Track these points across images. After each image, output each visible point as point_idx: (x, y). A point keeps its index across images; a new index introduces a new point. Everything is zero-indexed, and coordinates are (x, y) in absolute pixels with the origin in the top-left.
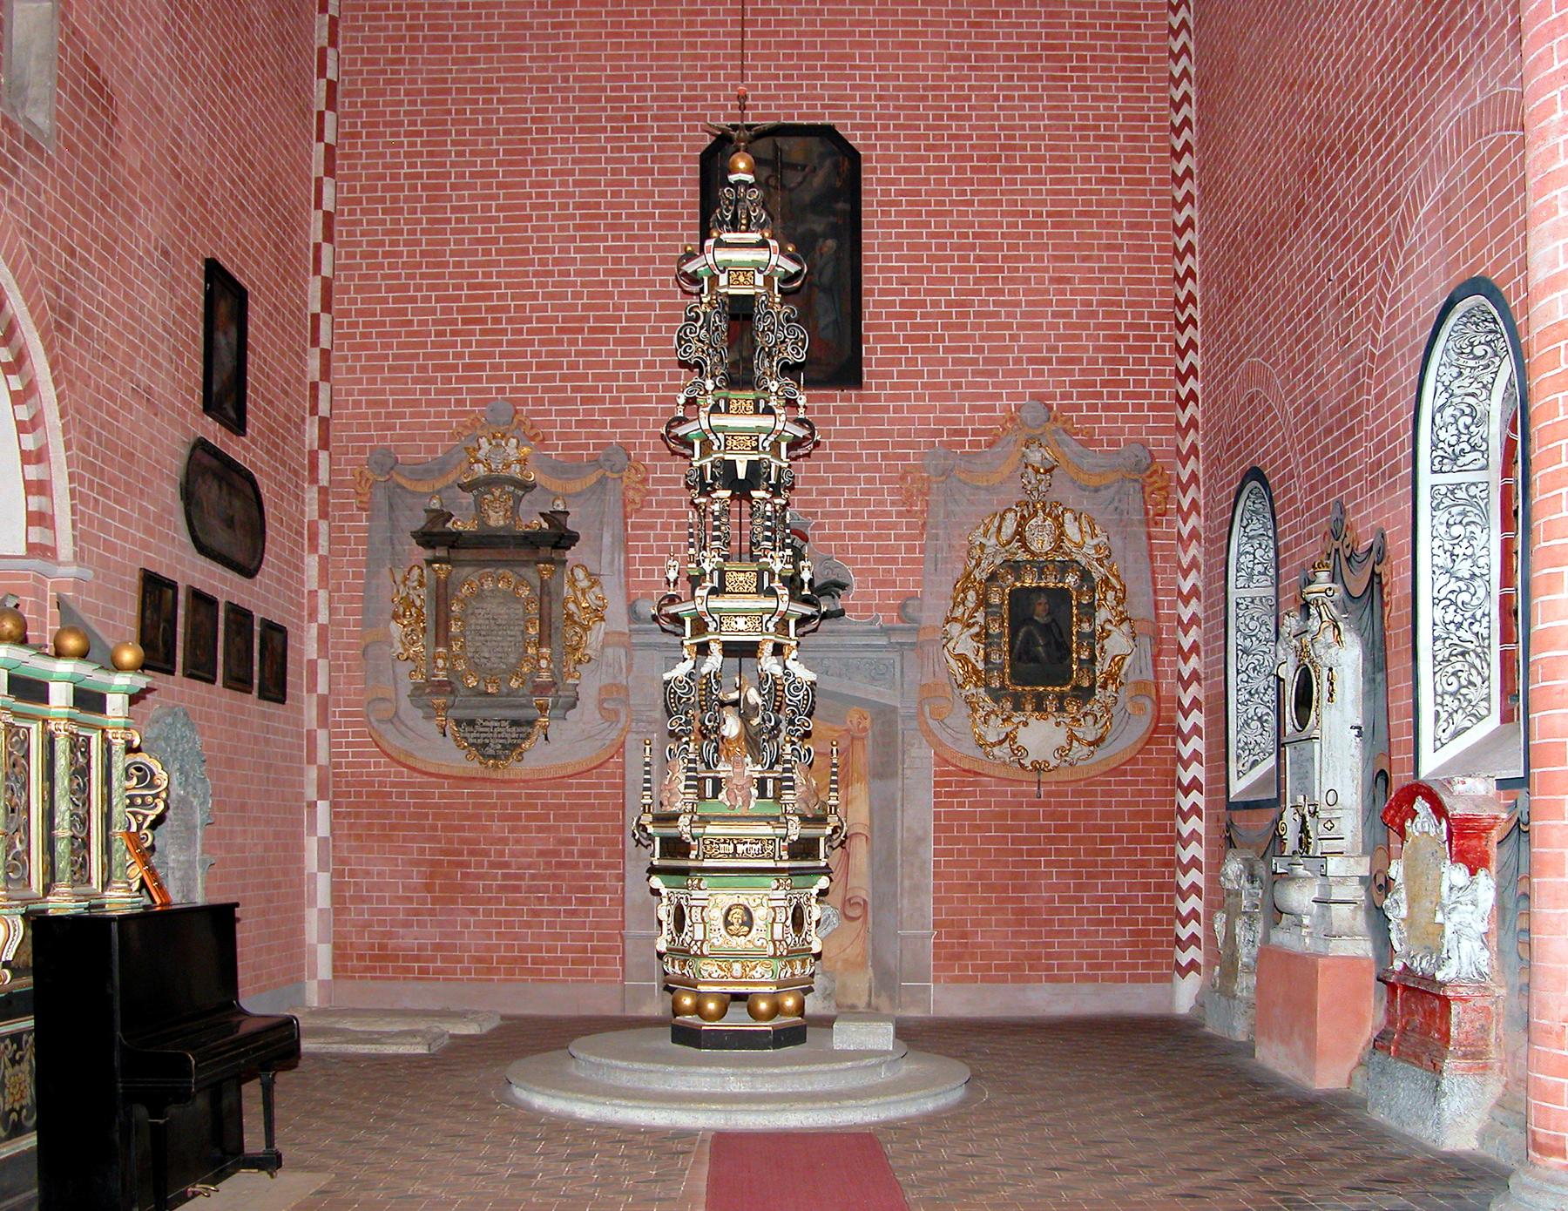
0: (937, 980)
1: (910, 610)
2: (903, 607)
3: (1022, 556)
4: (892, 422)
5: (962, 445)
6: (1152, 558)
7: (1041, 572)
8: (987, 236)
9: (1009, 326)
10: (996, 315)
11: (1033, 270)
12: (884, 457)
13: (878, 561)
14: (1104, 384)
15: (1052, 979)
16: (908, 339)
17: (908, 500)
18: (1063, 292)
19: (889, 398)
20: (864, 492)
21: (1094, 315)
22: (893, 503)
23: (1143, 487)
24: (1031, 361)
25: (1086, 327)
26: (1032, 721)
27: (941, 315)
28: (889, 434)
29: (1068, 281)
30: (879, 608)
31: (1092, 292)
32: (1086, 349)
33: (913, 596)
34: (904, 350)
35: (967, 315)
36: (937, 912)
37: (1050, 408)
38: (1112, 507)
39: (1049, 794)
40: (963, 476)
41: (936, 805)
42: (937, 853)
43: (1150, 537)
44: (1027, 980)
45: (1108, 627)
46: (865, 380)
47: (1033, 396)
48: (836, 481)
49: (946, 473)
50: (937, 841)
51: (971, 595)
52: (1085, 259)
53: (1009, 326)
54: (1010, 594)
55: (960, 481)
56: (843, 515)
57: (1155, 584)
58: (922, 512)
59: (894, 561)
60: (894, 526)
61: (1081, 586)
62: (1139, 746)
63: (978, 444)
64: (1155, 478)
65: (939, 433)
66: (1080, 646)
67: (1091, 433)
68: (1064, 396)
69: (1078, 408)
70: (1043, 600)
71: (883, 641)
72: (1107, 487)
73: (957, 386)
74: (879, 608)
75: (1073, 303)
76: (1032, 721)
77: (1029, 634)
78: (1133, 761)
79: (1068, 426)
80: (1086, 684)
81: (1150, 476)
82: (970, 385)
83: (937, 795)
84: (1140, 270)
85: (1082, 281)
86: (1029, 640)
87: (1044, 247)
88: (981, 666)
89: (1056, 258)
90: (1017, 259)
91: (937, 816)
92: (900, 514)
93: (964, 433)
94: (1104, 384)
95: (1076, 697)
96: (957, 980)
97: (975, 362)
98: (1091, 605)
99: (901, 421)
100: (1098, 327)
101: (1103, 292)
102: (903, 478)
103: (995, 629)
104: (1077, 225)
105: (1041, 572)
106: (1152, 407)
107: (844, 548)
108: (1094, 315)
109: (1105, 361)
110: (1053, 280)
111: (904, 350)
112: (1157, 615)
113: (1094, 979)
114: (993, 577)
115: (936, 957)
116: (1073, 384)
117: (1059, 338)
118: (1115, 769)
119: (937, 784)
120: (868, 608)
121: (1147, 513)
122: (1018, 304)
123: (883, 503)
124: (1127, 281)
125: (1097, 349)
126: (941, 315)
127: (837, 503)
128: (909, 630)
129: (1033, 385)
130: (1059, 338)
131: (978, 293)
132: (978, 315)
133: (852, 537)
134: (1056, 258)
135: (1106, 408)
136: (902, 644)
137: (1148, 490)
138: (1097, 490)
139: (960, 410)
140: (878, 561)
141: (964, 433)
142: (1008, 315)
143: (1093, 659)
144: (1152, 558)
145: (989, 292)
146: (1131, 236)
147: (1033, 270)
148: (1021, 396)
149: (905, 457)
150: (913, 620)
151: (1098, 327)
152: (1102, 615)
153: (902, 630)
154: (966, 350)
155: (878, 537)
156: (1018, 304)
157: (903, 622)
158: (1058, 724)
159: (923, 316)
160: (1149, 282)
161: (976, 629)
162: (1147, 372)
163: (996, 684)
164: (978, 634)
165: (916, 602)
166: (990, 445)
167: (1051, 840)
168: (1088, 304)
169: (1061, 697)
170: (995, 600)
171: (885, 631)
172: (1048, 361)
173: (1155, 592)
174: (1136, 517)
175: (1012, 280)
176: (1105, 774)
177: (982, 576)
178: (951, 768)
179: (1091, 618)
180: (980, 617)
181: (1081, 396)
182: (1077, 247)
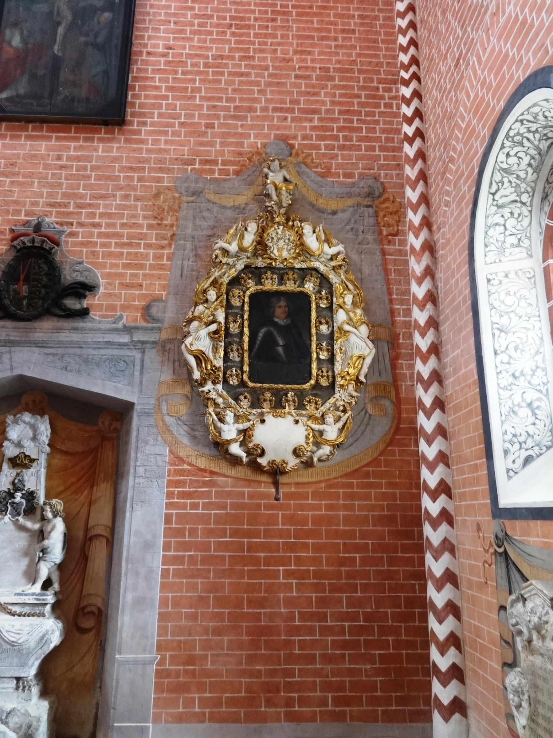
0: (157, 719)
1: (154, 311)
2: (146, 311)
3: (260, 263)
4: (148, 151)
5: (212, 172)
6: (386, 271)
7: (281, 280)
8: (242, 19)
9: (258, 84)
10: (248, 75)
11: (279, 44)
12: (140, 179)
13: (126, 266)
14: (340, 129)
15: (292, 717)
16: (169, 89)
17: (159, 217)
18: (305, 61)
19: (149, 133)
20: (119, 207)
21: (332, 79)
22: (145, 217)
23: (376, 214)
24: (275, 110)
25: (324, 87)
26: (269, 418)
27: (200, 73)
28: (147, 161)
29: (309, 53)
30: (124, 308)
31: (329, 61)
32: (324, 103)
33: (158, 299)
34: (166, 98)
35: (222, 74)
36: (162, 630)
37: (292, 146)
38: (348, 227)
39: (289, 496)
40: (211, 197)
41: (169, 506)
42: (166, 561)
43: (384, 253)
44: (263, 719)
45: (347, 327)
46: (129, 118)
47: (277, 137)
48: (93, 197)
49: (197, 193)
50: (167, 546)
51: (212, 295)
52: (323, 38)
53: (258, 84)
54: (251, 297)
55: (209, 201)
56: (97, 225)
57: (390, 294)
58: (172, 226)
59: (141, 267)
60: (142, 237)
61: (320, 292)
62: (381, 447)
63: (227, 173)
64: (386, 205)
65: (191, 162)
66: (319, 347)
67: (328, 168)
68: (304, 138)
69: (318, 147)
70: (283, 303)
71: (125, 339)
72: (344, 211)
73: (210, 126)
74: (124, 308)
75: (314, 69)
76: (269, 418)
77: (269, 336)
78: (375, 462)
79: (308, 160)
80: (324, 382)
81: (384, 202)
82: (221, 125)
83: (170, 495)
84: (369, 48)
85: (320, 53)
86: (269, 339)
87: (289, 28)
88: (219, 363)
89: (299, 37)
90: (266, 36)
91: (168, 519)
92: (150, 227)
93: (215, 162)
94: (340, 129)
95: (315, 395)
96: (180, 719)
97: (227, 109)
98: (330, 308)
99: (160, 151)
100: (335, 87)
101: (338, 62)
102: (156, 196)
103: (234, 328)
104: (315, 14)
105: (281, 280)
106: (382, 149)
107: (94, 254)
108: (332, 79)
109: (341, 112)
110: (296, 52)
111: (166, 98)
112: (393, 323)
113: (339, 717)
114: (235, 282)
115: (159, 687)
116: (313, 128)
117: (300, 93)
118: (356, 470)
119: (170, 483)
120: (113, 308)
121: (380, 233)
122: (266, 68)
123: (134, 216)
124: (359, 55)
125: (333, 103)
126: (200, 73)
127: (93, 215)
128: (152, 329)
129: (278, 128)
130: (300, 93)
131: (233, 58)
132: (230, 74)
133: (103, 245)
134: (299, 37)
135: (342, 148)
136: (143, 343)
137: (381, 214)
138: (334, 213)
139: (212, 144)
140: (126, 266)
141: (215, 162)
142: (257, 75)
143: (332, 360)
144: (386, 271)
145: (242, 58)
146: (362, 24)
147: (279, 44)
148: (267, 136)
149: (159, 180)
150: (156, 320)
151: (335, 87)
152: (341, 316)
153: (146, 329)
154: (220, 99)
155: (129, 245)
156: (266, 68)
157: (147, 321)
158: (297, 422)
159: (183, 73)
160: (377, 56)
161: (214, 327)
162: (377, 122)
163: (234, 381)
164: (216, 332)
165: (161, 304)
166: (237, 173)
167: (291, 547)
168: (328, 70)
169: (301, 395)
170: (236, 302)
171: (127, 329)
172: (292, 111)
173: (391, 301)
174: (370, 237)
175: (261, 51)
176: (346, 475)
177: (226, 280)
178: (186, 467)
179: (330, 322)
180: (221, 316)
181: (321, 138)
182: (318, 30)
